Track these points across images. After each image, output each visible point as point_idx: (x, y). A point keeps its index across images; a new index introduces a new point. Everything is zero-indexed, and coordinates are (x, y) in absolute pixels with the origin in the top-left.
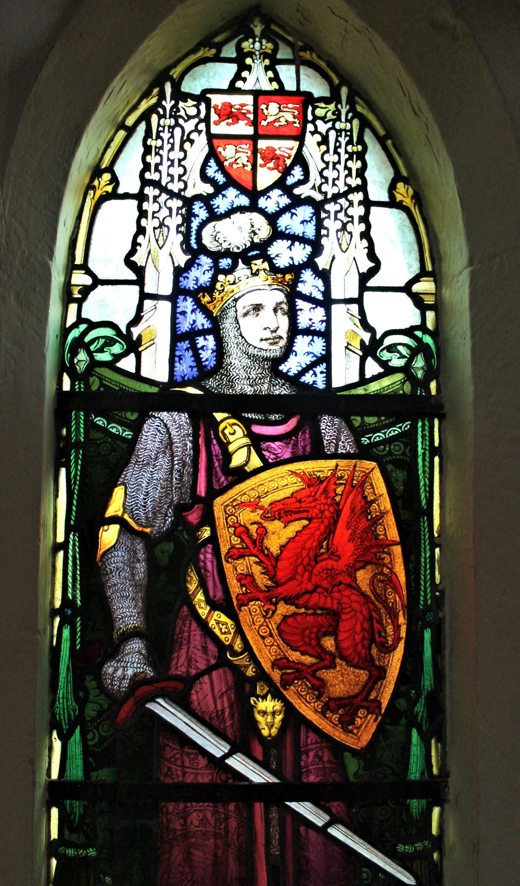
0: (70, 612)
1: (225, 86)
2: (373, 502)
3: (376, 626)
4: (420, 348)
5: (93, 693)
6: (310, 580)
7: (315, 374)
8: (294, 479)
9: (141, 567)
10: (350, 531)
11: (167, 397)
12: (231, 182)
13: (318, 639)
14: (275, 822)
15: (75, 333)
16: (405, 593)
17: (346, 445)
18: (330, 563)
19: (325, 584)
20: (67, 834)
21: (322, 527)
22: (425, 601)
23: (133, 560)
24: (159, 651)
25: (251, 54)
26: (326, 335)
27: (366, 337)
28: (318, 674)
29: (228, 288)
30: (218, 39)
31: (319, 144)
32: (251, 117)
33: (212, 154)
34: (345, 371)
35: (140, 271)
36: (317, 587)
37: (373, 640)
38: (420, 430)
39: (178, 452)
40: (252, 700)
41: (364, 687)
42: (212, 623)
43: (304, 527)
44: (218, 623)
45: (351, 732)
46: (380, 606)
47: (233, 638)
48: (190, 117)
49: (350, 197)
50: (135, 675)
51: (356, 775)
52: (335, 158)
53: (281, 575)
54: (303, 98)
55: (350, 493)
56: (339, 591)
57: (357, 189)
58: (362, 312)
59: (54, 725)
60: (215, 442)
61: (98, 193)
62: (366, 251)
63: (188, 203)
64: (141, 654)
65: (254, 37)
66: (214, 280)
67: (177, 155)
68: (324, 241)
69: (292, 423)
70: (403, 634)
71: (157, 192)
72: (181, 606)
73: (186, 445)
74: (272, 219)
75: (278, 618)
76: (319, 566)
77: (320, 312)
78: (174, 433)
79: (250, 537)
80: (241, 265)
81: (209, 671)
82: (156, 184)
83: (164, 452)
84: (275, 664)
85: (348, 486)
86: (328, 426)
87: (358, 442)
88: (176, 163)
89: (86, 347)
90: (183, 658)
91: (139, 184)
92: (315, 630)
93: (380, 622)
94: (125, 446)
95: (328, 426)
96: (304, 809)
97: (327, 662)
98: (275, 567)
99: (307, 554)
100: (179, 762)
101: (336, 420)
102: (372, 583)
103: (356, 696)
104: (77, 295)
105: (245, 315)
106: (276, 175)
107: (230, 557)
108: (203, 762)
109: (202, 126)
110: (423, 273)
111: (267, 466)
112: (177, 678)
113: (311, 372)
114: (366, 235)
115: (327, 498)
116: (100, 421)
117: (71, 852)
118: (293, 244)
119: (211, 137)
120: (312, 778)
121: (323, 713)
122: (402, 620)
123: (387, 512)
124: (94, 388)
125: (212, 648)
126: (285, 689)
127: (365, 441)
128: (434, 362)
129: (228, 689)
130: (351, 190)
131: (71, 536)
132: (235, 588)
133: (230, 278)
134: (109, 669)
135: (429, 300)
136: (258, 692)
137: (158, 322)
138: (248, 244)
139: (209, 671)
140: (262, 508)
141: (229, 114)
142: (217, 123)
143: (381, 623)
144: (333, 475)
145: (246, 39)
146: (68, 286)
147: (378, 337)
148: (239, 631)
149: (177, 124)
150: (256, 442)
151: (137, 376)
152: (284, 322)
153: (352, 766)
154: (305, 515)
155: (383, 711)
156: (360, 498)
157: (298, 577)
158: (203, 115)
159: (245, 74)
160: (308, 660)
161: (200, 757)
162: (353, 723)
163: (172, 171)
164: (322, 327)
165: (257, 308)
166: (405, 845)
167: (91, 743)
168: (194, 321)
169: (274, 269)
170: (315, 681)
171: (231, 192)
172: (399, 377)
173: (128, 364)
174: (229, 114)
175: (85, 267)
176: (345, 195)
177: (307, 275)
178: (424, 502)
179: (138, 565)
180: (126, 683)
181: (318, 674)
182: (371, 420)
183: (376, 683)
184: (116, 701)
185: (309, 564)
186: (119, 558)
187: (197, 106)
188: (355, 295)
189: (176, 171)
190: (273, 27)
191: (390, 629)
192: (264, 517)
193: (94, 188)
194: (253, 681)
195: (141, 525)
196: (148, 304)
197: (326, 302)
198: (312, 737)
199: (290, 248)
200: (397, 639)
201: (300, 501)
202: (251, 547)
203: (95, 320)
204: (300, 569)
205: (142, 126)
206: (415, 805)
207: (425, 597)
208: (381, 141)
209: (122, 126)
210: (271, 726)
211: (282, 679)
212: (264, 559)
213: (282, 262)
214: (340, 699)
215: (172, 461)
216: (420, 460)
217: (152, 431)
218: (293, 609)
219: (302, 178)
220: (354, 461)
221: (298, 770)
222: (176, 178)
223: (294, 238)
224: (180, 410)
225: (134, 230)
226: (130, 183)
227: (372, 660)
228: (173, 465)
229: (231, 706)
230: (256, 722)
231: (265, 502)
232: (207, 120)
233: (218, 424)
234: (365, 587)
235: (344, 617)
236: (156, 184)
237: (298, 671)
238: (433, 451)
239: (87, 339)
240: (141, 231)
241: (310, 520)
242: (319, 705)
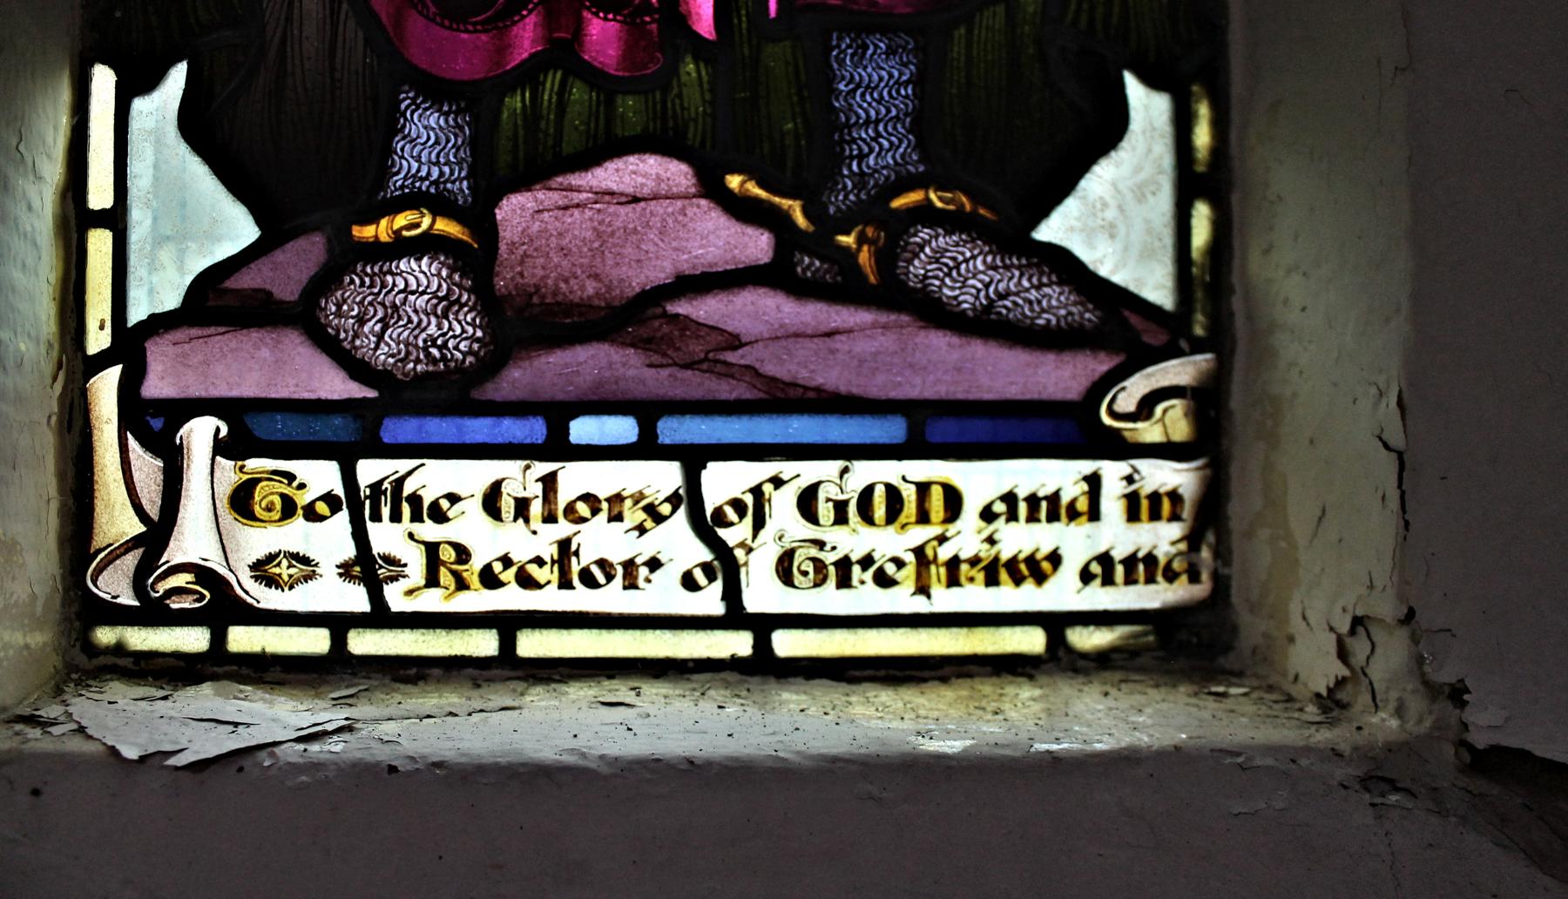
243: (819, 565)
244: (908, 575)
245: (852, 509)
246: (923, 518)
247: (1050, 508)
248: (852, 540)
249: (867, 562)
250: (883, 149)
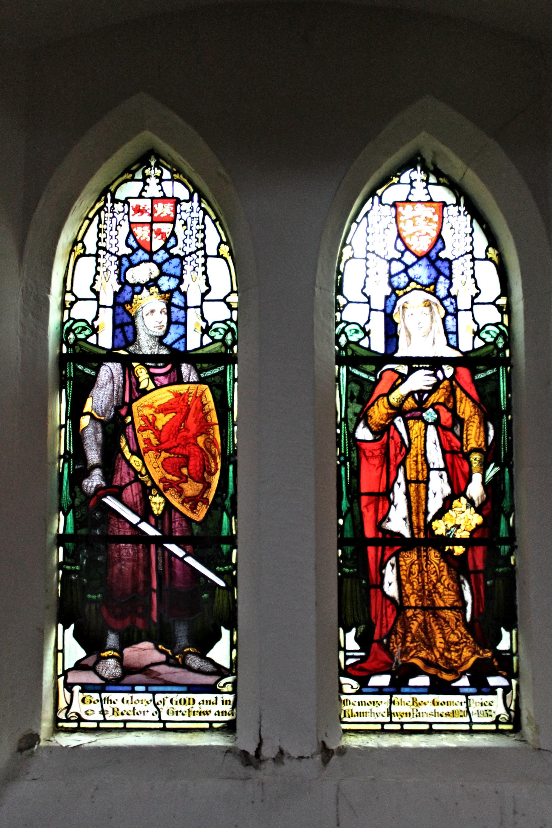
0: (68, 457)
1: (137, 195)
2: (206, 404)
3: (206, 463)
4: (230, 330)
5: (78, 494)
6: (176, 441)
7: (179, 343)
8: (169, 394)
9: (100, 436)
10: (195, 418)
11: (110, 356)
12: (140, 247)
13: (180, 469)
14: (160, 554)
15: (68, 325)
16: (220, 447)
17: (194, 377)
18: (185, 433)
19: (183, 443)
20: (66, 559)
21: (182, 416)
22: (230, 451)
23: (96, 433)
25: (149, 177)
26: (185, 324)
27: (204, 325)
28: (180, 485)
29: (139, 302)
30: (134, 168)
31: (183, 225)
32: (150, 211)
33: (131, 232)
35: (97, 293)
36: (179, 444)
37: (205, 470)
38: (228, 370)
39: (116, 381)
40: (150, 497)
41: (201, 491)
42: (132, 462)
43: (174, 417)
44: (135, 461)
45: (195, 513)
46: (208, 454)
47: (142, 469)
48: (120, 212)
49: (198, 253)
50: (97, 485)
51: (197, 533)
52: (191, 233)
53: (163, 439)
54: (175, 200)
55: (194, 400)
56: (189, 446)
57: (201, 249)
58: (202, 312)
59: (61, 508)
60: (133, 376)
61: (77, 254)
62: (205, 281)
63: (120, 258)
64: (99, 475)
65: (151, 166)
66: (132, 298)
67: (114, 233)
68: (184, 277)
69: (169, 367)
70: (219, 467)
71: (104, 253)
72: (118, 454)
73: (119, 378)
74: (160, 266)
75: (161, 459)
76: (180, 435)
77: (182, 312)
78: (114, 372)
79: (149, 421)
80: (145, 289)
81: (130, 483)
82: (104, 249)
83: (110, 382)
84: (160, 481)
85: (194, 397)
86: (185, 369)
87: (199, 376)
88: (114, 237)
89: (73, 331)
90: (119, 478)
91: (96, 248)
92: (178, 464)
93: (208, 461)
94: (91, 379)
95: (185, 369)
96: (173, 548)
97: (183, 480)
98: (160, 435)
99: (174, 429)
100: (117, 526)
101: (189, 366)
102: (204, 443)
103: (197, 496)
104: (68, 306)
105: (147, 315)
106: (162, 243)
107: (140, 430)
108: (127, 526)
109: (126, 217)
110: (232, 291)
111: (157, 388)
112: (116, 487)
113: (178, 343)
114: (205, 273)
115: (184, 403)
116: (80, 367)
117: (68, 567)
118: (170, 278)
119: (130, 223)
120: (177, 534)
121: (182, 504)
122: (219, 460)
123: (212, 409)
124: (78, 351)
125: (132, 472)
126: (165, 492)
127: (202, 375)
128: (236, 337)
129: (139, 492)
130: (198, 249)
131: (68, 421)
132: (142, 445)
133: (140, 296)
134: (85, 482)
135: (235, 306)
136: (153, 493)
138: (148, 280)
139: (130, 483)
140: (154, 407)
141: (139, 210)
142: (133, 215)
143: (209, 462)
144: (187, 392)
145: (147, 168)
146: (63, 302)
147: (210, 325)
148: (144, 465)
149: (114, 217)
150: (152, 376)
151: (97, 346)
152: (165, 318)
153: (196, 529)
154: (174, 411)
155: (210, 503)
156: (199, 403)
157: (170, 440)
158: (126, 212)
159: (146, 188)
160: (175, 479)
161: (126, 524)
162: (196, 508)
163: (112, 241)
164: (183, 320)
165: (152, 311)
166: (220, 567)
167: (77, 517)
168: (123, 318)
169: (161, 292)
170: (178, 489)
171: (140, 252)
172: (219, 344)
173: (92, 340)
174: (139, 210)
175: (71, 292)
176: (195, 252)
177: (176, 294)
178: (230, 405)
179: (98, 434)
180: (93, 489)
181: (180, 485)
182: (205, 365)
183: (206, 490)
184: (88, 497)
185: (175, 434)
186: (89, 432)
187: (123, 206)
188: (199, 304)
189: (114, 241)
190: (161, 160)
191: (213, 465)
192: (155, 412)
193: (74, 251)
194: (150, 488)
195: (99, 416)
196: (101, 309)
197: (185, 308)
198: (178, 515)
199: (168, 281)
200: (216, 469)
201: (171, 404)
202: (149, 425)
203: (77, 318)
204: (171, 436)
205: (97, 218)
206: (225, 548)
207: (230, 450)
208: (214, 222)
209: (87, 218)
210: (158, 509)
211: (164, 488)
212: (155, 432)
213: (164, 288)
214: (190, 497)
215: (114, 386)
216: (228, 384)
217: (104, 372)
218: (168, 455)
219: (174, 243)
220: (197, 385)
221: (171, 529)
222: (114, 245)
223: (170, 275)
224: (117, 362)
225: (94, 272)
226: (91, 249)
227: (204, 479)
228: (114, 388)
229: (140, 500)
230: (151, 508)
231: (156, 405)
232: (128, 214)
233: (134, 368)
234: (201, 444)
235: (191, 459)
236: (104, 249)
237: (171, 484)
238: (235, 380)
239: (74, 328)
240: (97, 273)
241: (176, 413)
242: (180, 500)
243: (173, 712)
244: (187, 714)
245: (178, 702)
246: (189, 704)
247: (209, 702)
248: (178, 707)
249: (180, 711)
250: (182, 641)
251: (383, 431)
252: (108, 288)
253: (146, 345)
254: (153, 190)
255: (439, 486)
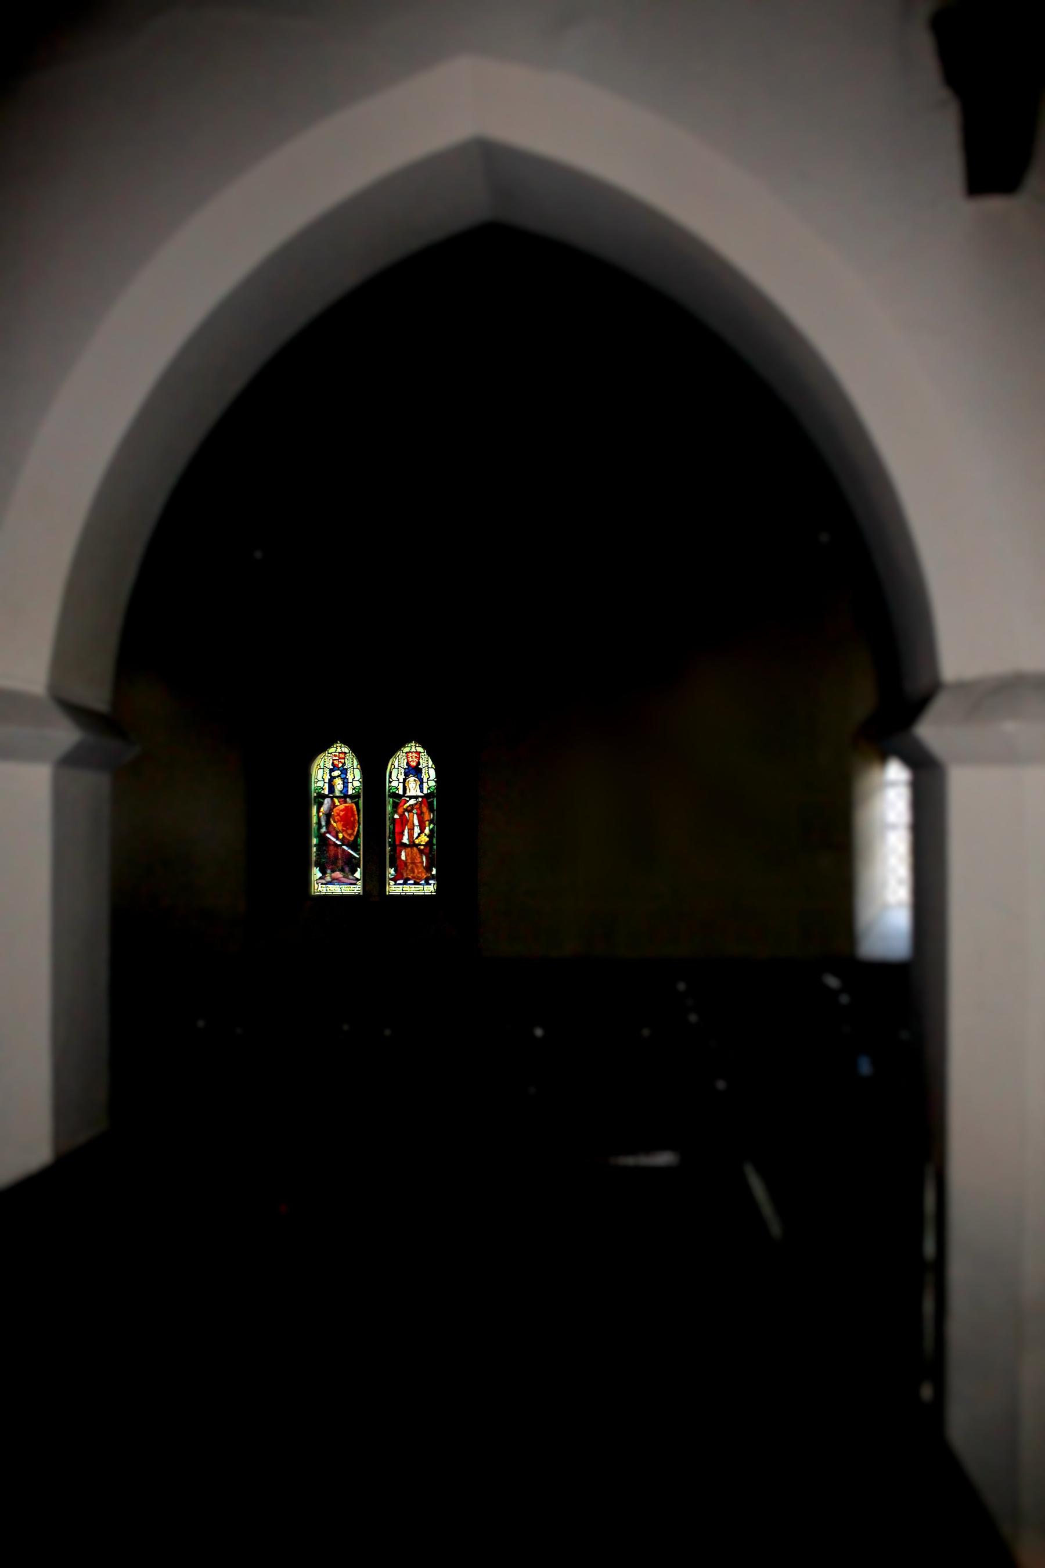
24: (327, 828)
34: (350, 792)
137: (327, 786)
251: (402, 816)
252: (327, 777)
253: (337, 794)
254: (339, 750)
255: (417, 830)
